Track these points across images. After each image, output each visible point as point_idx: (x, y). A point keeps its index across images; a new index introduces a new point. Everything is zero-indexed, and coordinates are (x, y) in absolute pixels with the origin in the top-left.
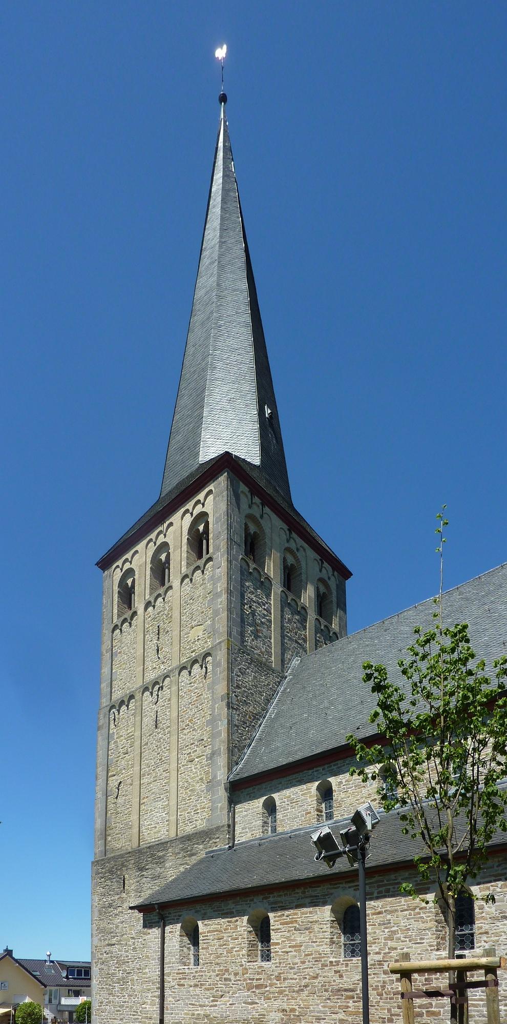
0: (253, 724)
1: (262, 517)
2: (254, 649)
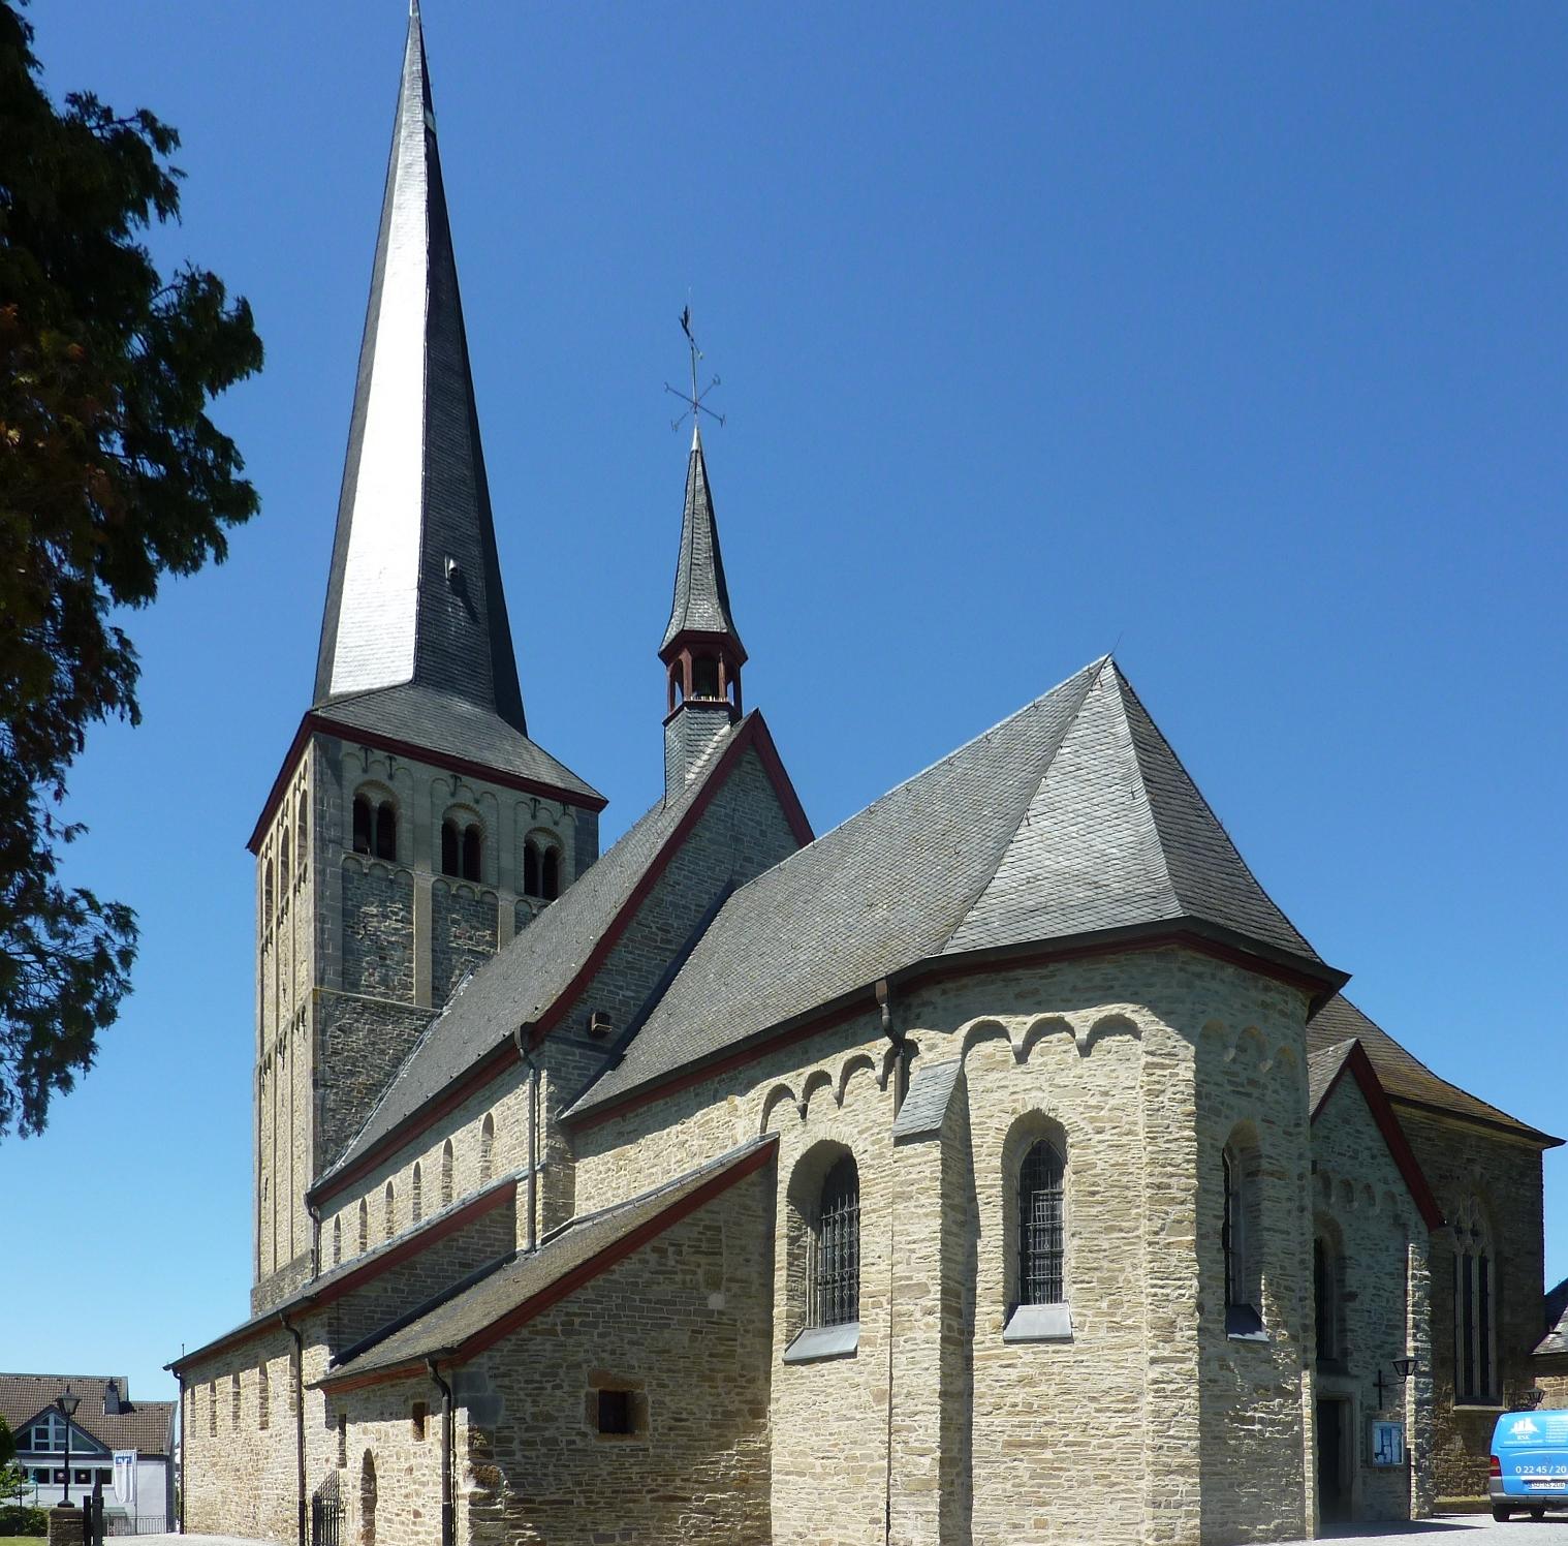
0: (366, 1100)
1: (391, 777)
2: (374, 987)
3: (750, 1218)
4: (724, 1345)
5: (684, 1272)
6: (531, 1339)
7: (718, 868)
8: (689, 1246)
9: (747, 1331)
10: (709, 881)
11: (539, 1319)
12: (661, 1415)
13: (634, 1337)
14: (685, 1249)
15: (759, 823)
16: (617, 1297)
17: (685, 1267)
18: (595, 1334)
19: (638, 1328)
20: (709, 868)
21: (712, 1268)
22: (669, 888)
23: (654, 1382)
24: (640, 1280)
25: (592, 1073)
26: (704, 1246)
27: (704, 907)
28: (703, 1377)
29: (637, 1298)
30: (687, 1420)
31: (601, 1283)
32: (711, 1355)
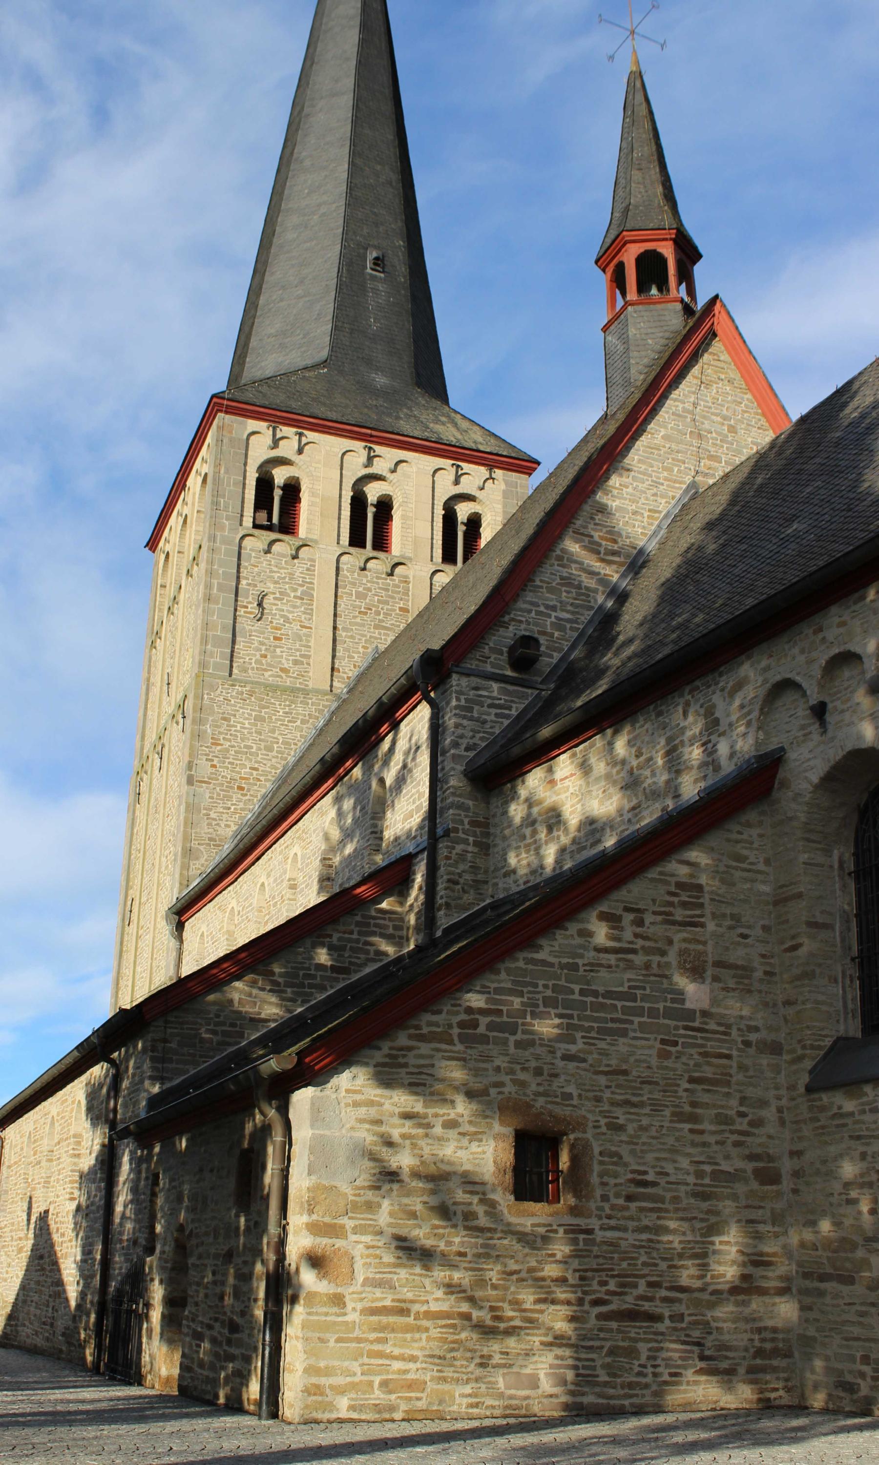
3: (745, 874)
4: (709, 1064)
6: (410, 1049)
7: (676, 469)
8: (654, 913)
9: (747, 1044)
10: (666, 483)
11: (427, 1017)
12: (616, 1176)
13: (573, 1049)
14: (649, 918)
15: (725, 418)
16: (546, 986)
17: (648, 944)
18: (511, 1044)
19: (579, 1035)
20: (665, 469)
21: (692, 947)
23: (603, 1121)
24: (580, 962)
25: (514, 713)
26: (679, 914)
27: (660, 512)
28: (679, 1116)
29: (576, 988)
30: (654, 1184)
31: (521, 964)
32: (691, 1080)
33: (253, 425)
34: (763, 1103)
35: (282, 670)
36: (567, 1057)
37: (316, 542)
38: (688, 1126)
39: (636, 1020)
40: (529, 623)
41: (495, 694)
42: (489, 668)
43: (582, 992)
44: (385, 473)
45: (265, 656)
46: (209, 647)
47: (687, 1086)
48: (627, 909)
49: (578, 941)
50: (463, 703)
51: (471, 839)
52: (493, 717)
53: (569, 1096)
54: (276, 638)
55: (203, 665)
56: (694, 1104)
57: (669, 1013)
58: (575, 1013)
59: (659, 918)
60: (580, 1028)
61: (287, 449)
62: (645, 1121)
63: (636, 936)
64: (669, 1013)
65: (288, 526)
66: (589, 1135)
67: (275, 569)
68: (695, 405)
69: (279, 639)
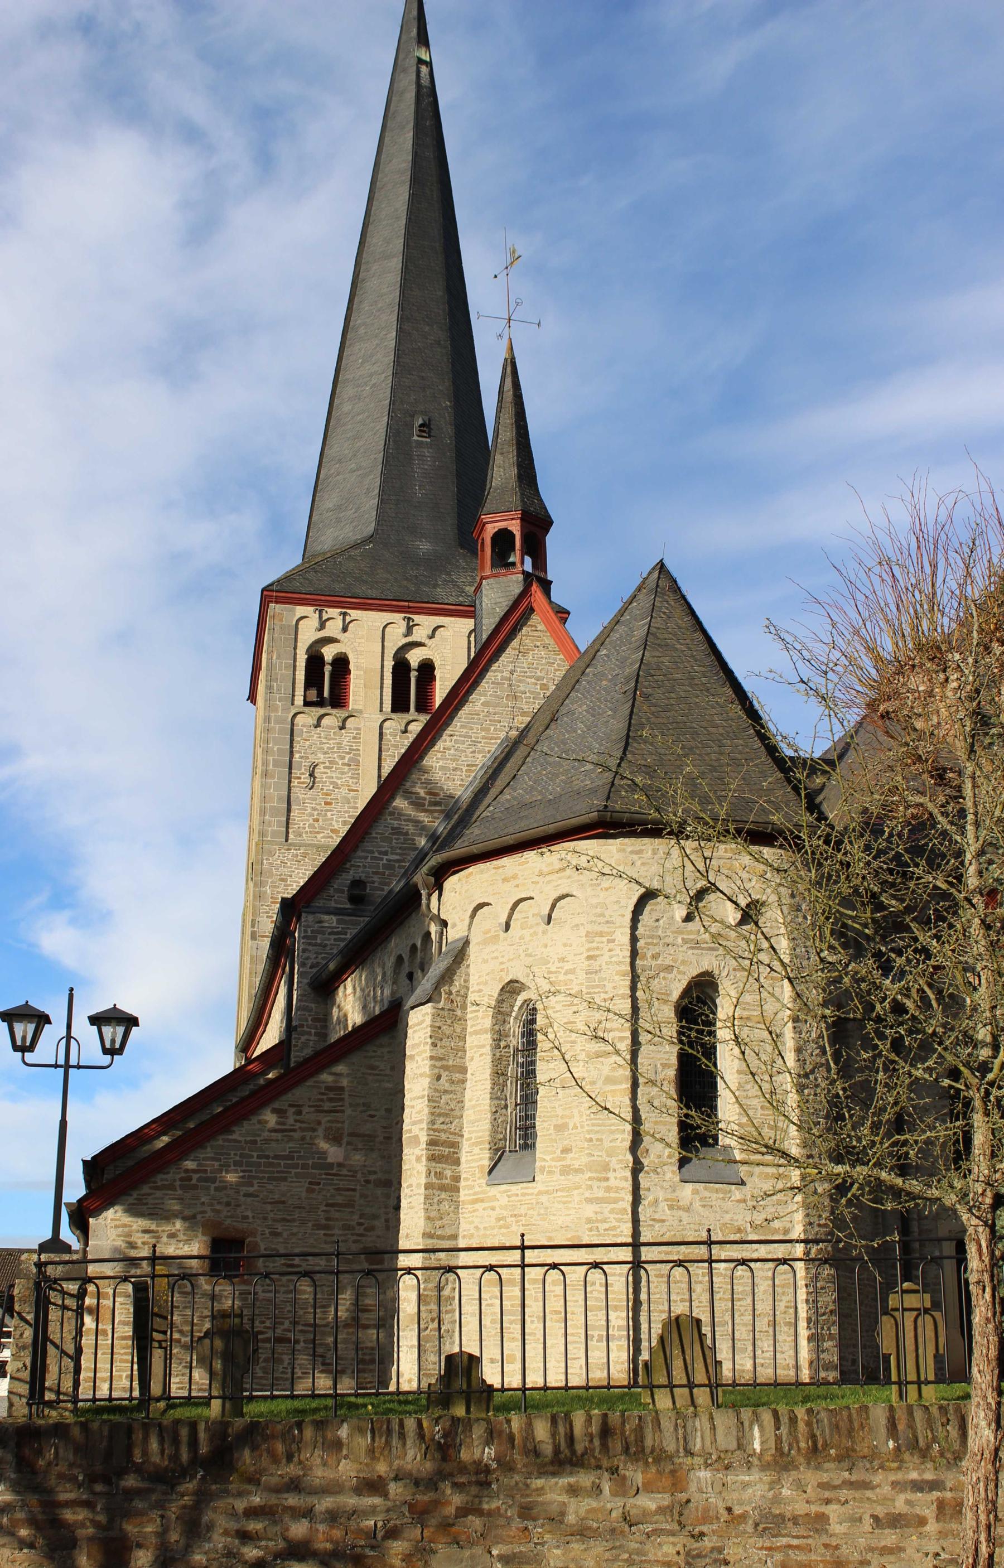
4: (340, 1195)
5: (302, 1130)
8: (309, 1106)
9: (368, 1182)
11: (160, 1176)
13: (251, 1190)
16: (235, 1154)
17: (303, 1125)
18: (212, 1189)
19: (255, 1182)
20: (482, 729)
21: (334, 1125)
22: (439, 755)
24: (258, 1139)
25: (349, 936)
26: (327, 1106)
27: (476, 765)
28: (318, 1226)
29: (255, 1154)
31: (220, 1142)
32: (327, 1205)
33: (300, 610)
34: (375, 1217)
35: (332, 831)
36: (245, 1195)
37: (360, 711)
38: (323, 1232)
39: (293, 1171)
40: (365, 867)
41: (334, 924)
42: (333, 904)
43: (258, 1157)
44: (424, 640)
45: (317, 820)
46: (267, 817)
47: (325, 1208)
48: (291, 1106)
49: (258, 1126)
50: (309, 933)
51: (313, 1031)
52: (332, 942)
53: (247, 1217)
54: (326, 803)
55: (262, 834)
56: (328, 1219)
57: (315, 1166)
58: (254, 1169)
59: (312, 1109)
60: (255, 1177)
61: (333, 629)
62: (295, 1230)
63: (296, 1121)
64: (315, 1166)
65: (338, 699)
66: (258, 1239)
67: (325, 741)
68: (512, 673)
69: (329, 804)
